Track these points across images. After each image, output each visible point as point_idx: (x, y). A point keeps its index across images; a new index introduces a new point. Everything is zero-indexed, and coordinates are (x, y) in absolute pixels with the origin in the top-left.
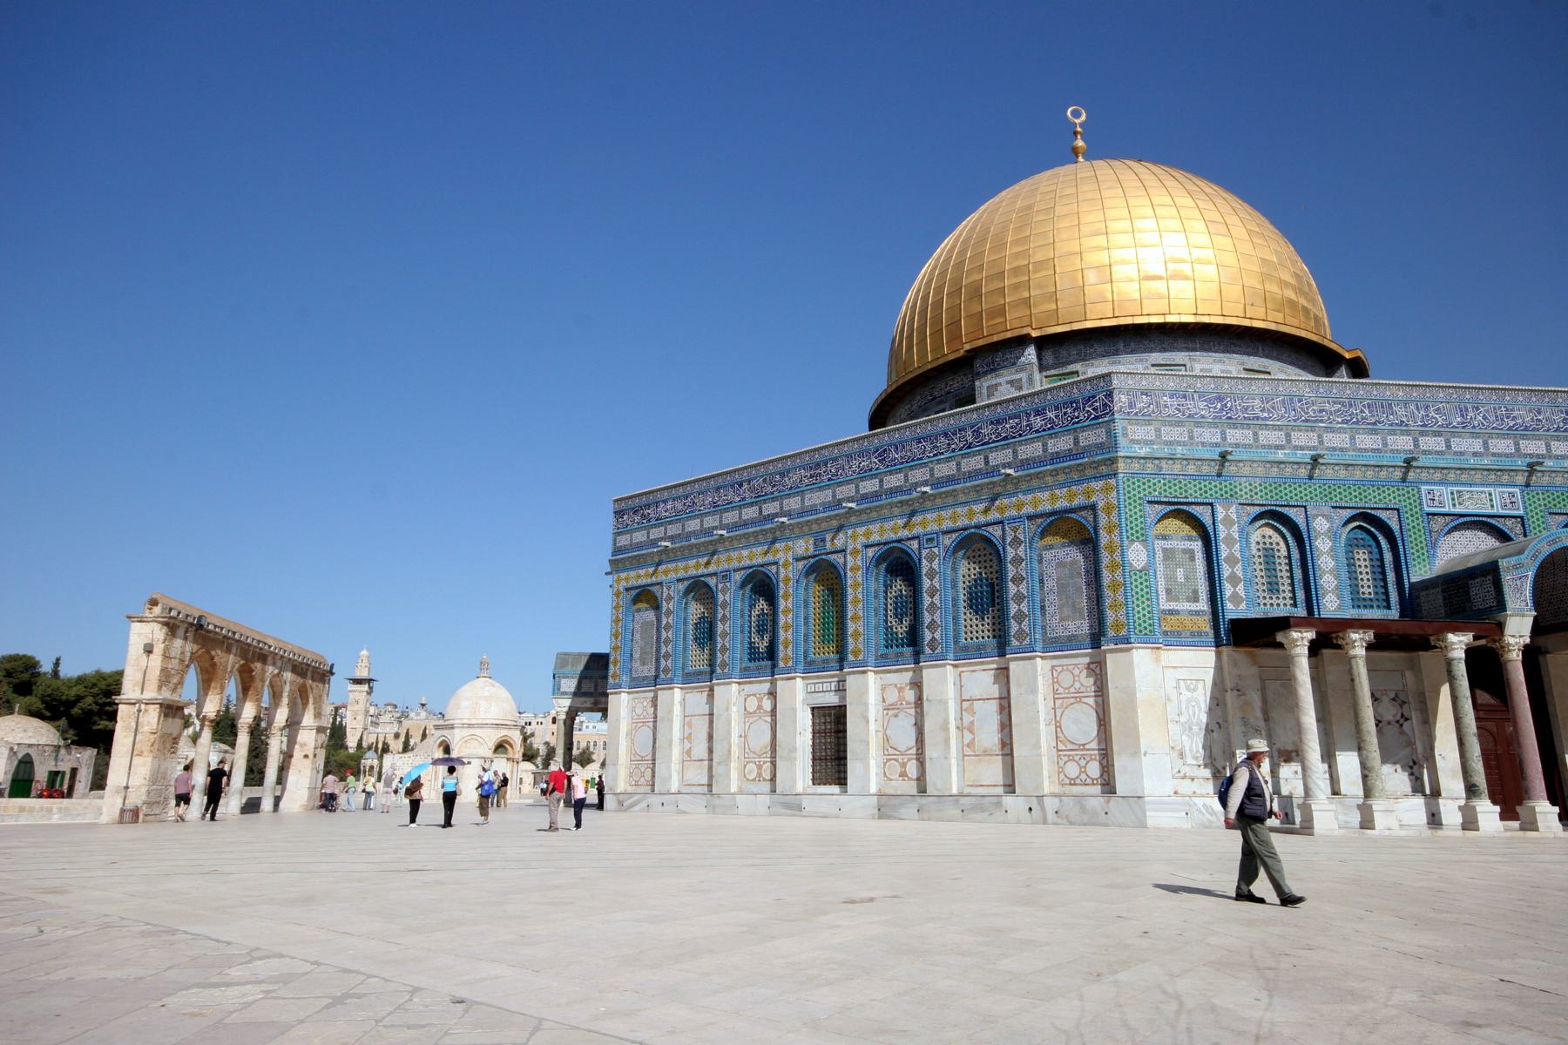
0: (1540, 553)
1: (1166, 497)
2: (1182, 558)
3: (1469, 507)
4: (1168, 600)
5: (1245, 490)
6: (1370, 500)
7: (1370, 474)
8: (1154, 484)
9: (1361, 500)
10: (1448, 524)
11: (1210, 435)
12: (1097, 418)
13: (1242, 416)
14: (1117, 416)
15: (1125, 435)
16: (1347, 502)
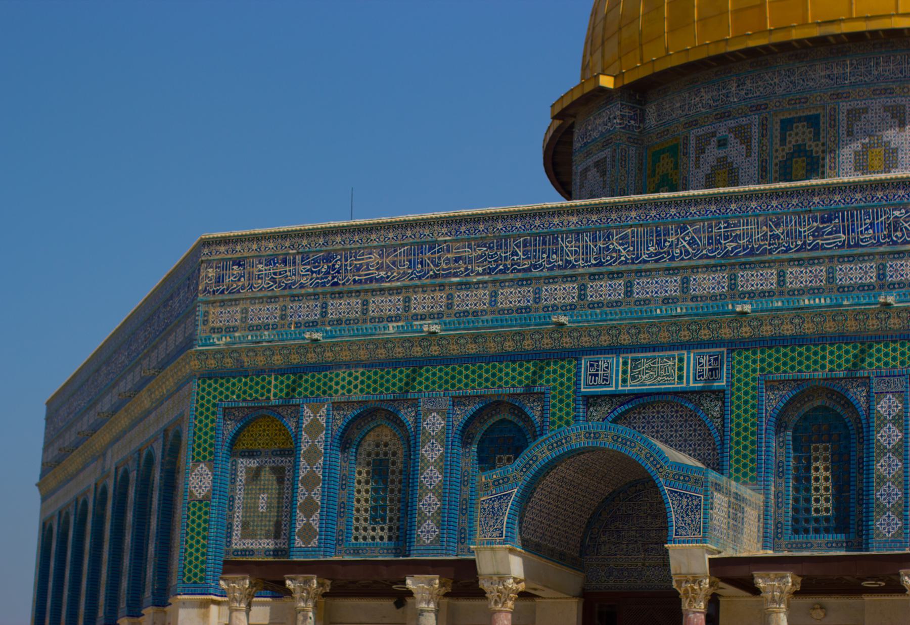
0: (534, 462)
1: (245, 400)
2: (268, 480)
3: (647, 383)
4: (244, 536)
5: (342, 383)
6: (507, 383)
7: (509, 346)
8: (234, 385)
9: (493, 384)
10: (616, 409)
11: (307, 310)
12: (193, 300)
13: (352, 279)
14: (201, 297)
15: (205, 322)
16: (473, 388)
